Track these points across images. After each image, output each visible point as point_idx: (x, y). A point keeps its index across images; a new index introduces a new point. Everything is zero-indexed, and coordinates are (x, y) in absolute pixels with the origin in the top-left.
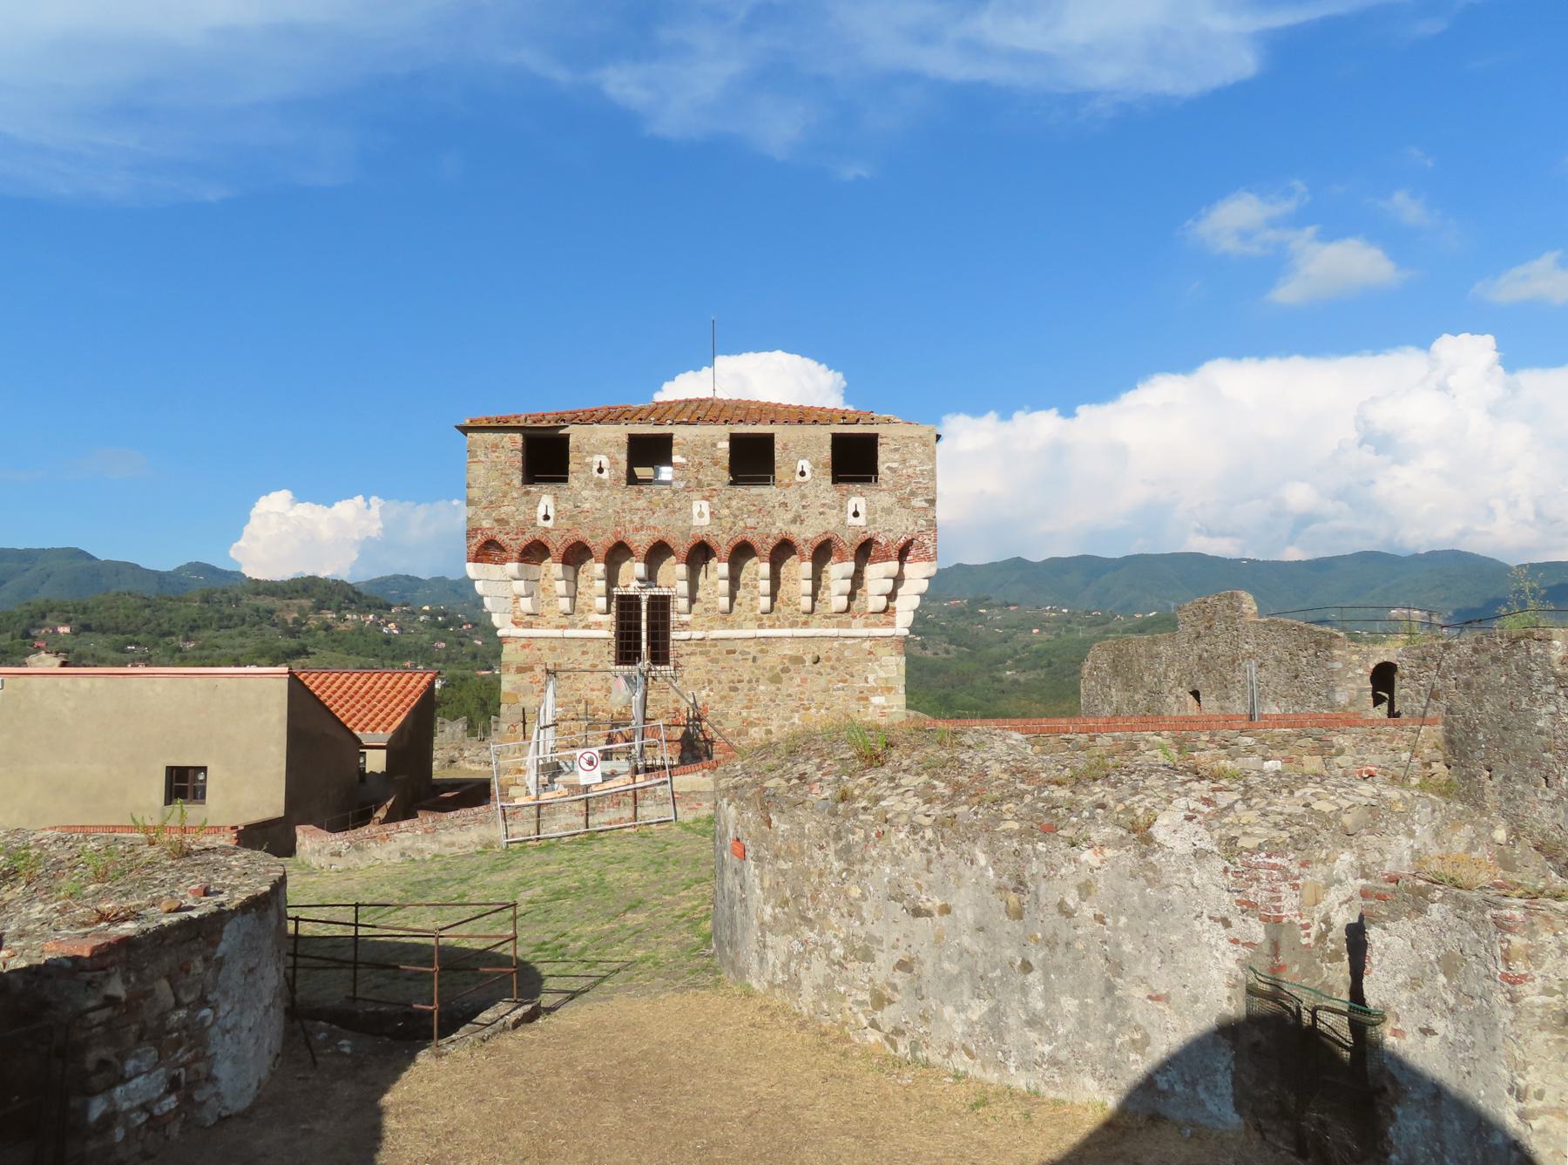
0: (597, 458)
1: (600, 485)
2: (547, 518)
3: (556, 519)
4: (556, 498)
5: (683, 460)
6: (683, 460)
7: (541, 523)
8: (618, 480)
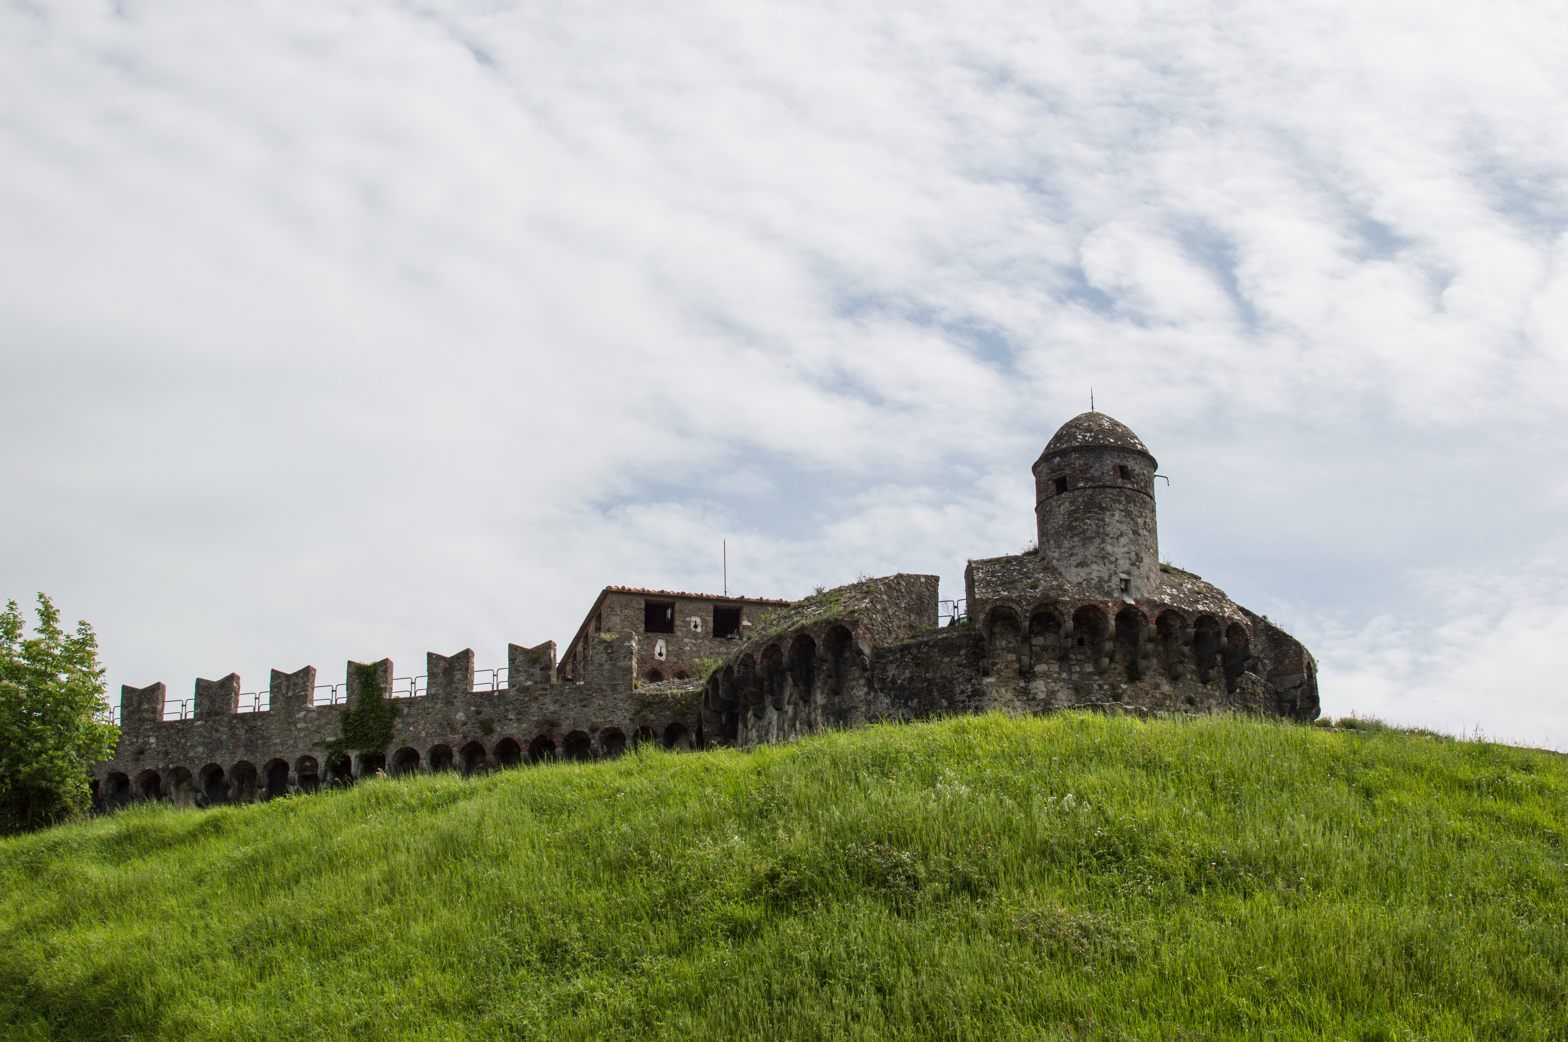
0: (693, 619)
1: (695, 636)
2: (661, 654)
3: (667, 656)
4: (667, 642)
5: (750, 624)
6: (750, 624)
7: (657, 657)
8: (707, 633)
